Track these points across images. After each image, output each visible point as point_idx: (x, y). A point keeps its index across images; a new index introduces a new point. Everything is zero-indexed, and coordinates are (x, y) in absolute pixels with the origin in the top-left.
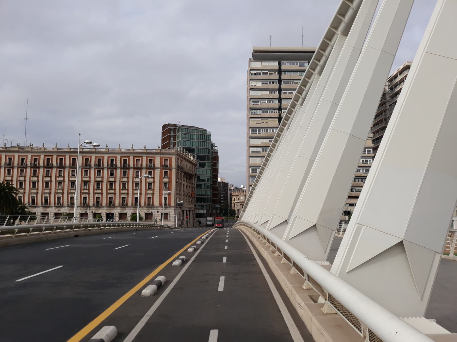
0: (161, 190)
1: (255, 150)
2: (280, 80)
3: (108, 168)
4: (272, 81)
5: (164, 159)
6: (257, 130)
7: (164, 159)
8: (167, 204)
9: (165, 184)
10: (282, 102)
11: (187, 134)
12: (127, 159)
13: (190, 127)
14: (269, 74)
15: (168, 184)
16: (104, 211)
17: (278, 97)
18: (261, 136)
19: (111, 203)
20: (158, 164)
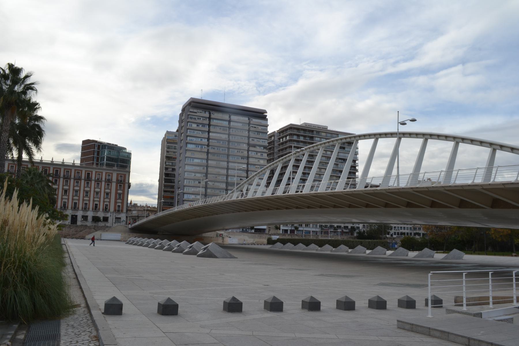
0: (116, 199)
1: (187, 174)
2: (209, 125)
3: (85, 180)
4: (203, 125)
5: (119, 175)
8: (120, 211)
9: (120, 194)
10: (210, 141)
12: (90, 173)
13: (110, 144)
14: (202, 119)
15: (122, 195)
16: (69, 212)
17: (207, 137)
19: (75, 207)
20: (114, 179)
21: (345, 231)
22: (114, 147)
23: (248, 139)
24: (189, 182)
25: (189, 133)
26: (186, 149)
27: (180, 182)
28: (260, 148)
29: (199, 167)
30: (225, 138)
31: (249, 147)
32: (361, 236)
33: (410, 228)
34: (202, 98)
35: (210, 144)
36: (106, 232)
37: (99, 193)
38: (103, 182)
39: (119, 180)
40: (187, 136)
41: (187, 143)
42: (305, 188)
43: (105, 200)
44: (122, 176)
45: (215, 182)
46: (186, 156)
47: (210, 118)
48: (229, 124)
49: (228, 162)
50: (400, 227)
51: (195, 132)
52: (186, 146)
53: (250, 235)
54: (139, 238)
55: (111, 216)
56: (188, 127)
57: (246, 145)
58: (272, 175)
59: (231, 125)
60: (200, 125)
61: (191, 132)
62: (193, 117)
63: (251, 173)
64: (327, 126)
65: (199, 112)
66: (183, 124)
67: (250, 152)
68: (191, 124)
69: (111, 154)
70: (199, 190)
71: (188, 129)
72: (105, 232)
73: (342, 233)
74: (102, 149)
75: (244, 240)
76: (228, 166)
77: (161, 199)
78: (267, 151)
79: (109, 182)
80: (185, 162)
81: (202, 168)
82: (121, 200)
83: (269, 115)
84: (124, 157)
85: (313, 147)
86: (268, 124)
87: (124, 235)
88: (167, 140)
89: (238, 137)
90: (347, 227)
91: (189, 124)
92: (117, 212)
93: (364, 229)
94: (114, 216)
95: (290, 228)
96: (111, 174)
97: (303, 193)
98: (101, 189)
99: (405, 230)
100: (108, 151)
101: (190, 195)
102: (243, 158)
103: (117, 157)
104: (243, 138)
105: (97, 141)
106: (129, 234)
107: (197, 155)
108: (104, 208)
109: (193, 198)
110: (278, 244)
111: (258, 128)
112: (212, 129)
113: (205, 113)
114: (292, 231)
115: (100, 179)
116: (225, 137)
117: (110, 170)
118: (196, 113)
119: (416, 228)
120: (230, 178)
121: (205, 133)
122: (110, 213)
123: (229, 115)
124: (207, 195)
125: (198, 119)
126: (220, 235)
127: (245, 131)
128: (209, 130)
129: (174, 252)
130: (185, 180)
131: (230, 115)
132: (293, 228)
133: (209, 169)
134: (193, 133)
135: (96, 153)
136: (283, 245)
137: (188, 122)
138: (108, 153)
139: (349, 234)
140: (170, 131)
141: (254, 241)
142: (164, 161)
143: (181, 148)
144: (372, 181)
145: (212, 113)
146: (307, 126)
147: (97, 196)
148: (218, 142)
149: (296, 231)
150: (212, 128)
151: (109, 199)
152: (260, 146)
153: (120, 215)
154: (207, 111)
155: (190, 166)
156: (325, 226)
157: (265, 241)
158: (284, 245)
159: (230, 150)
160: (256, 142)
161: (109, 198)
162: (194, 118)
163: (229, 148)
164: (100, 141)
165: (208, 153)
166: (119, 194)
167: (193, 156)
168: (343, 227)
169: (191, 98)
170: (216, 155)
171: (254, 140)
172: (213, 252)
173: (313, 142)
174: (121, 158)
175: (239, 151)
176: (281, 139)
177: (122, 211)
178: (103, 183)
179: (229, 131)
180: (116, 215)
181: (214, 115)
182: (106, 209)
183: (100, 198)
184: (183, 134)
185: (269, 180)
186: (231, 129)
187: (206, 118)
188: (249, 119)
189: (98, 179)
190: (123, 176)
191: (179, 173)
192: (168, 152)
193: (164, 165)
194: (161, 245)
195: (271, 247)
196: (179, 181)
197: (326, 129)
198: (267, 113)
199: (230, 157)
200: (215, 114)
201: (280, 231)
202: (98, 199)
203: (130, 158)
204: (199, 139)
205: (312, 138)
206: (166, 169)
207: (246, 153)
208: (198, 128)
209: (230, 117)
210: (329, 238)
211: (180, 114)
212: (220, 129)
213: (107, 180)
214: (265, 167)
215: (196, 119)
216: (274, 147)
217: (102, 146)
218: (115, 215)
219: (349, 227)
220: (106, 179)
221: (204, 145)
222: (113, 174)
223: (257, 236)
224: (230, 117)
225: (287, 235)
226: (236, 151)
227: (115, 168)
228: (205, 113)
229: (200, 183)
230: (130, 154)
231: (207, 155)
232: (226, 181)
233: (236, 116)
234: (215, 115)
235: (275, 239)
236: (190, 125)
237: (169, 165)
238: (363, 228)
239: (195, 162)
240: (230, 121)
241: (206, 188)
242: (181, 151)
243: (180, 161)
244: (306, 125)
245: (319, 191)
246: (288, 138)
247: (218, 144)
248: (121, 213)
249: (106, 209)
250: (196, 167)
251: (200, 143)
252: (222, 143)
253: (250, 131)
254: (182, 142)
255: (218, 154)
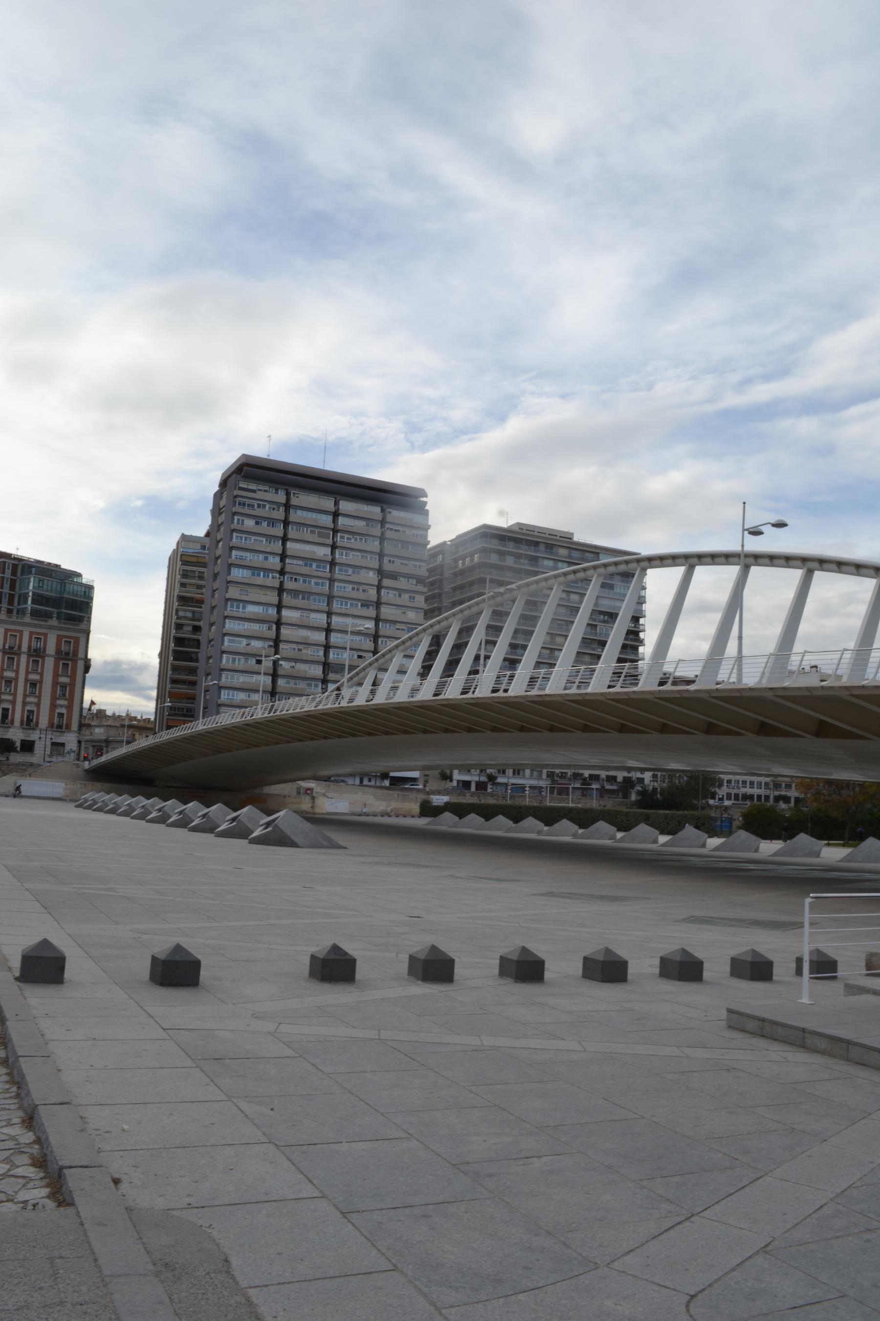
0: (54, 698)
1: (230, 641)
2: (286, 523)
4: (272, 522)
5: (64, 640)
6: (235, 604)
7: (64, 640)
9: (64, 686)
10: (287, 561)
11: (45, 581)
14: (270, 508)
17: (280, 552)
18: (247, 617)
20: (51, 649)
21: (608, 787)
22: (52, 570)
23: (379, 560)
24: (234, 660)
25: (235, 541)
26: (229, 579)
27: (211, 661)
28: (408, 581)
29: (258, 625)
30: (324, 555)
31: (382, 578)
32: (648, 800)
33: (767, 784)
34: (269, 456)
35: (288, 568)
36: (28, 778)
37: (13, 683)
38: (22, 655)
39: (62, 652)
40: (232, 548)
41: (230, 566)
42: (513, 682)
43: (28, 699)
44: (70, 642)
45: (296, 661)
46: (227, 597)
47: (287, 506)
48: (335, 521)
49: (329, 614)
50: (743, 781)
51: (251, 538)
52: (229, 573)
53: (379, 792)
54: (109, 794)
55: (40, 738)
56: (235, 525)
57: (374, 574)
58: (436, 648)
59: (339, 524)
60: (263, 523)
61: (242, 537)
62: (248, 501)
63: (386, 641)
64: (571, 532)
65: (261, 490)
66: (221, 519)
67: (383, 591)
68: (241, 518)
69: (45, 587)
70: (256, 680)
71: (233, 531)
72: (26, 776)
73: (602, 792)
74: (22, 575)
75: (365, 805)
76: (329, 624)
77: (164, 700)
78: (425, 590)
79: (37, 654)
80: (225, 612)
81: (265, 627)
82: (66, 699)
83: (432, 502)
84: (77, 594)
85: (537, 582)
86: (429, 524)
87: (72, 787)
88: (181, 555)
89: (355, 553)
90: (614, 778)
91: (236, 518)
92: (55, 729)
93: (656, 784)
94: (47, 740)
95: (476, 779)
96: (42, 637)
97: (511, 693)
98: (17, 672)
99: (753, 788)
100: (37, 580)
101: (236, 692)
102: (365, 604)
103: (59, 596)
104: (367, 557)
105: (11, 555)
106: (85, 785)
107: (254, 595)
108: (25, 719)
109: (242, 700)
110: (447, 815)
111: (405, 532)
112: (292, 533)
113: (277, 490)
114: (481, 786)
115: (16, 647)
116: (323, 552)
117: (41, 626)
118: (254, 491)
119: (781, 784)
120: (334, 655)
121: (274, 542)
122: (38, 732)
123: (336, 498)
124: (276, 693)
125: (258, 507)
126: (306, 792)
127: (373, 541)
128: (285, 534)
129: (194, 829)
130: (224, 655)
131: (338, 499)
132: (483, 779)
133: (285, 632)
134: (245, 540)
135: (7, 584)
136: (458, 818)
137: (234, 514)
138: (36, 585)
139: (618, 795)
140: (189, 534)
141: (387, 807)
142: (175, 608)
143: (216, 576)
144: (678, 670)
145: (294, 493)
146: (524, 531)
147: (8, 690)
148: (306, 565)
149: (489, 786)
150: (292, 529)
151: (36, 696)
152: (408, 576)
153: (62, 738)
154: (285, 487)
155: (237, 622)
156: (560, 775)
157: (416, 808)
158: (460, 818)
159: (336, 584)
160: (396, 566)
161: (37, 694)
162: (249, 505)
163: (332, 581)
164: (18, 554)
165: (281, 590)
166: (61, 686)
167: (244, 598)
168: (605, 777)
169: (244, 455)
170: (301, 597)
171: (393, 562)
172: (288, 832)
173: (536, 569)
174: (69, 598)
175: (356, 587)
176: (461, 562)
177: (68, 727)
178: (24, 658)
179: (333, 539)
180: (53, 737)
181: (298, 497)
182: (29, 721)
183: (15, 695)
184: (221, 543)
185: (428, 661)
186: (339, 534)
187: (278, 504)
188: (383, 511)
189: (11, 648)
190: (72, 641)
191: (211, 638)
192: (183, 585)
193: (175, 617)
194: (161, 813)
195: (428, 824)
196: (209, 658)
197: (571, 539)
198: (426, 496)
199: (335, 601)
200: (300, 496)
201: (451, 783)
202: (11, 698)
203: (91, 599)
204: (261, 557)
205: (535, 560)
206: (179, 627)
207: (373, 592)
208: (258, 529)
209: (336, 504)
210: (571, 805)
211: (216, 495)
212: (313, 532)
213: (32, 650)
214: (420, 628)
215: (253, 506)
216: (441, 581)
217: (23, 566)
218: (50, 737)
219: (620, 779)
220: (29, 647)
221: (273, 571)
222: (49, 635)
223: (396, 795)
224: (336, 504)
225: (469, 794)
226: (350, 589)
227: (54, 622)
228: (277, 493)
229: (259, 662)
230: (90, 588)
231: (280, 595)
232: (323, 659)
233: (350, 501)
234: (301, 498)
235: (439, 804)
236: (238, 520)
237: (185, 618)
238: (653, 781)
239: (249, 612)
240: (336, 515)
241: (275, 676)
242: (216, 585)
243: (213, 608)
244: (520, 529)
245: (549, 690)
246: (476, 558)
247: (305, 570)
248: (64, 732)
249: (29, 721)
250: (252, 624)
251: (264, 567)
252: (316, 568)
253: (385, 539)
254: (219, 561)
255: (306, 594)
